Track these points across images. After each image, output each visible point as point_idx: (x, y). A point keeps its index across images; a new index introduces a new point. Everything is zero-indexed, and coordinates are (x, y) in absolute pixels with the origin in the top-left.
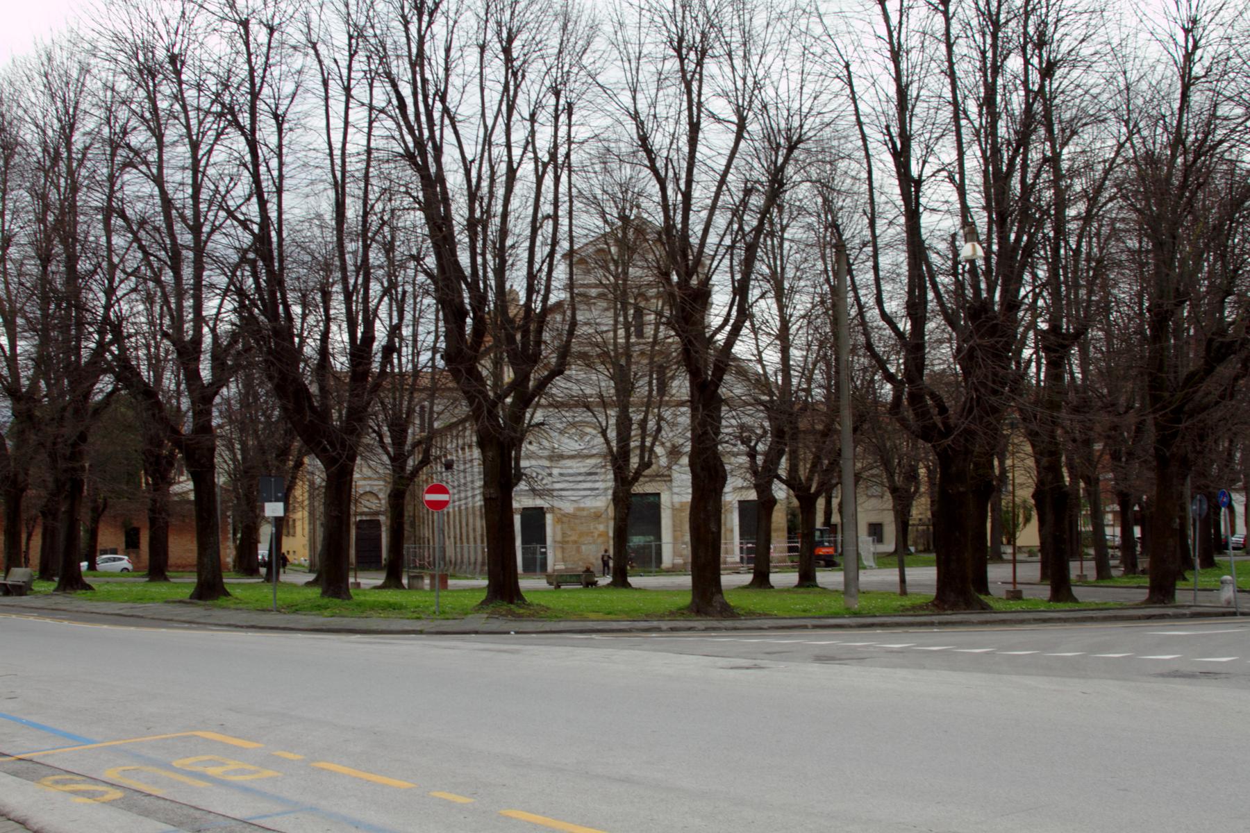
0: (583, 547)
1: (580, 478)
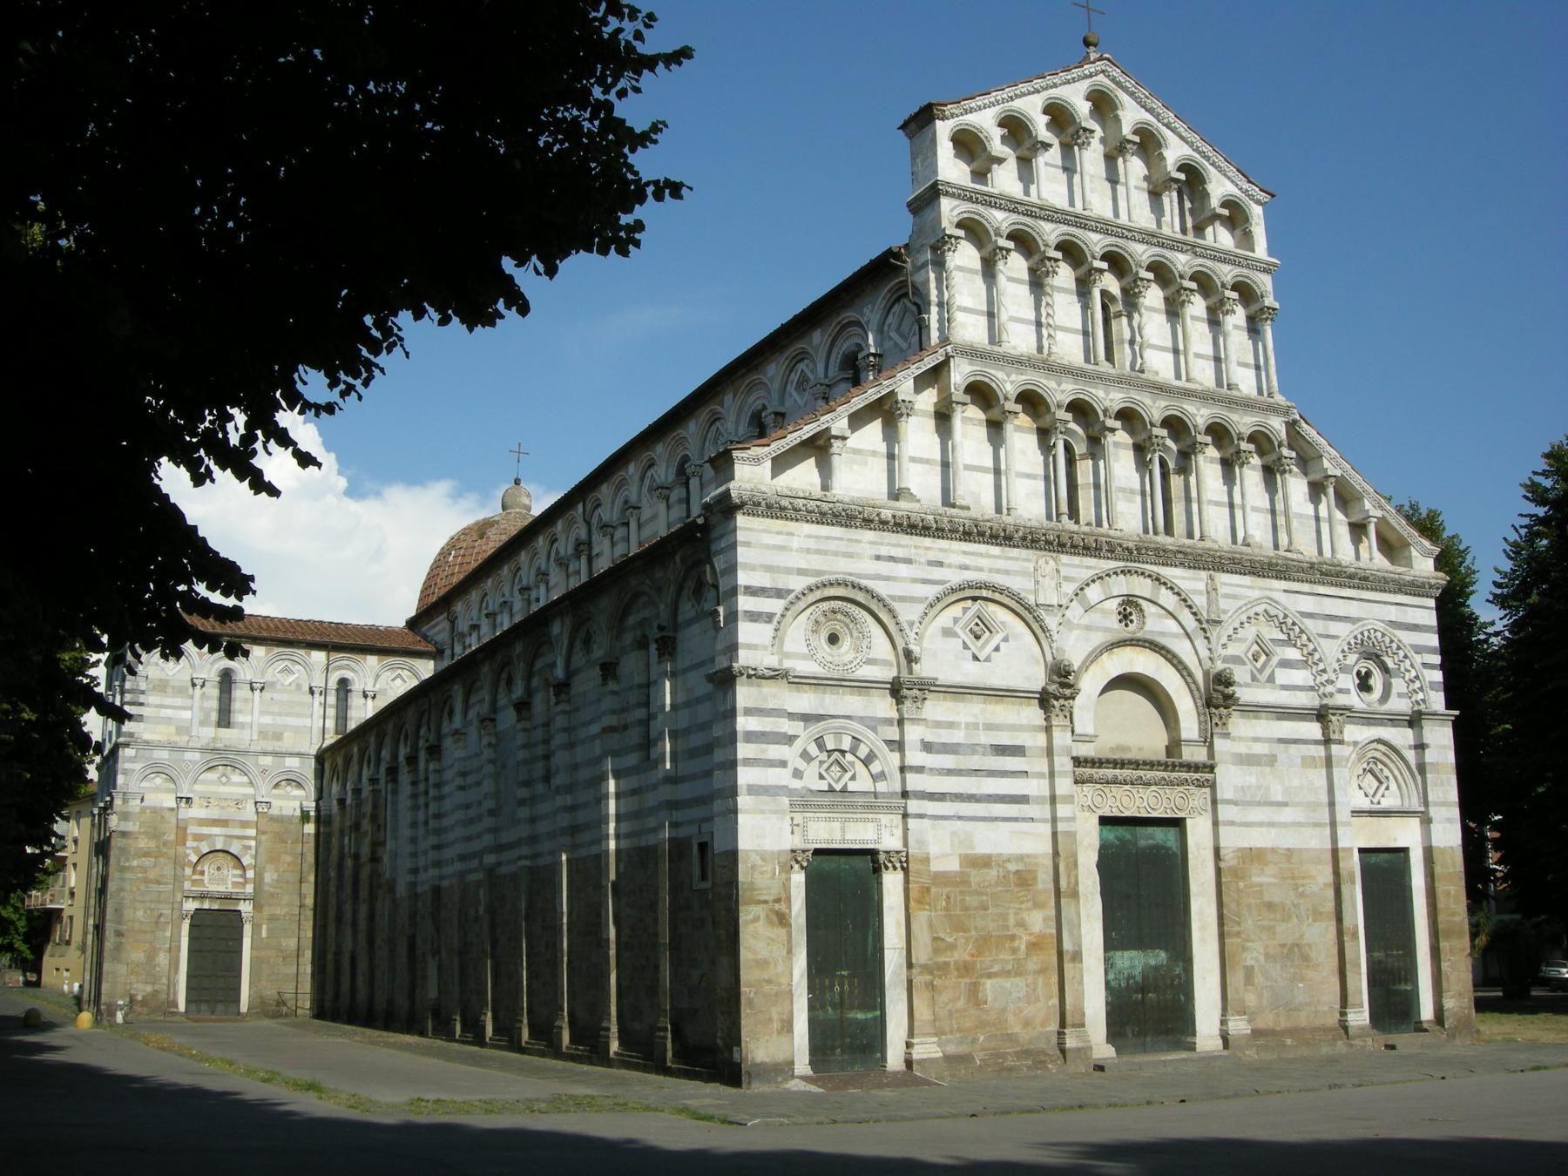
0: (989, 985)
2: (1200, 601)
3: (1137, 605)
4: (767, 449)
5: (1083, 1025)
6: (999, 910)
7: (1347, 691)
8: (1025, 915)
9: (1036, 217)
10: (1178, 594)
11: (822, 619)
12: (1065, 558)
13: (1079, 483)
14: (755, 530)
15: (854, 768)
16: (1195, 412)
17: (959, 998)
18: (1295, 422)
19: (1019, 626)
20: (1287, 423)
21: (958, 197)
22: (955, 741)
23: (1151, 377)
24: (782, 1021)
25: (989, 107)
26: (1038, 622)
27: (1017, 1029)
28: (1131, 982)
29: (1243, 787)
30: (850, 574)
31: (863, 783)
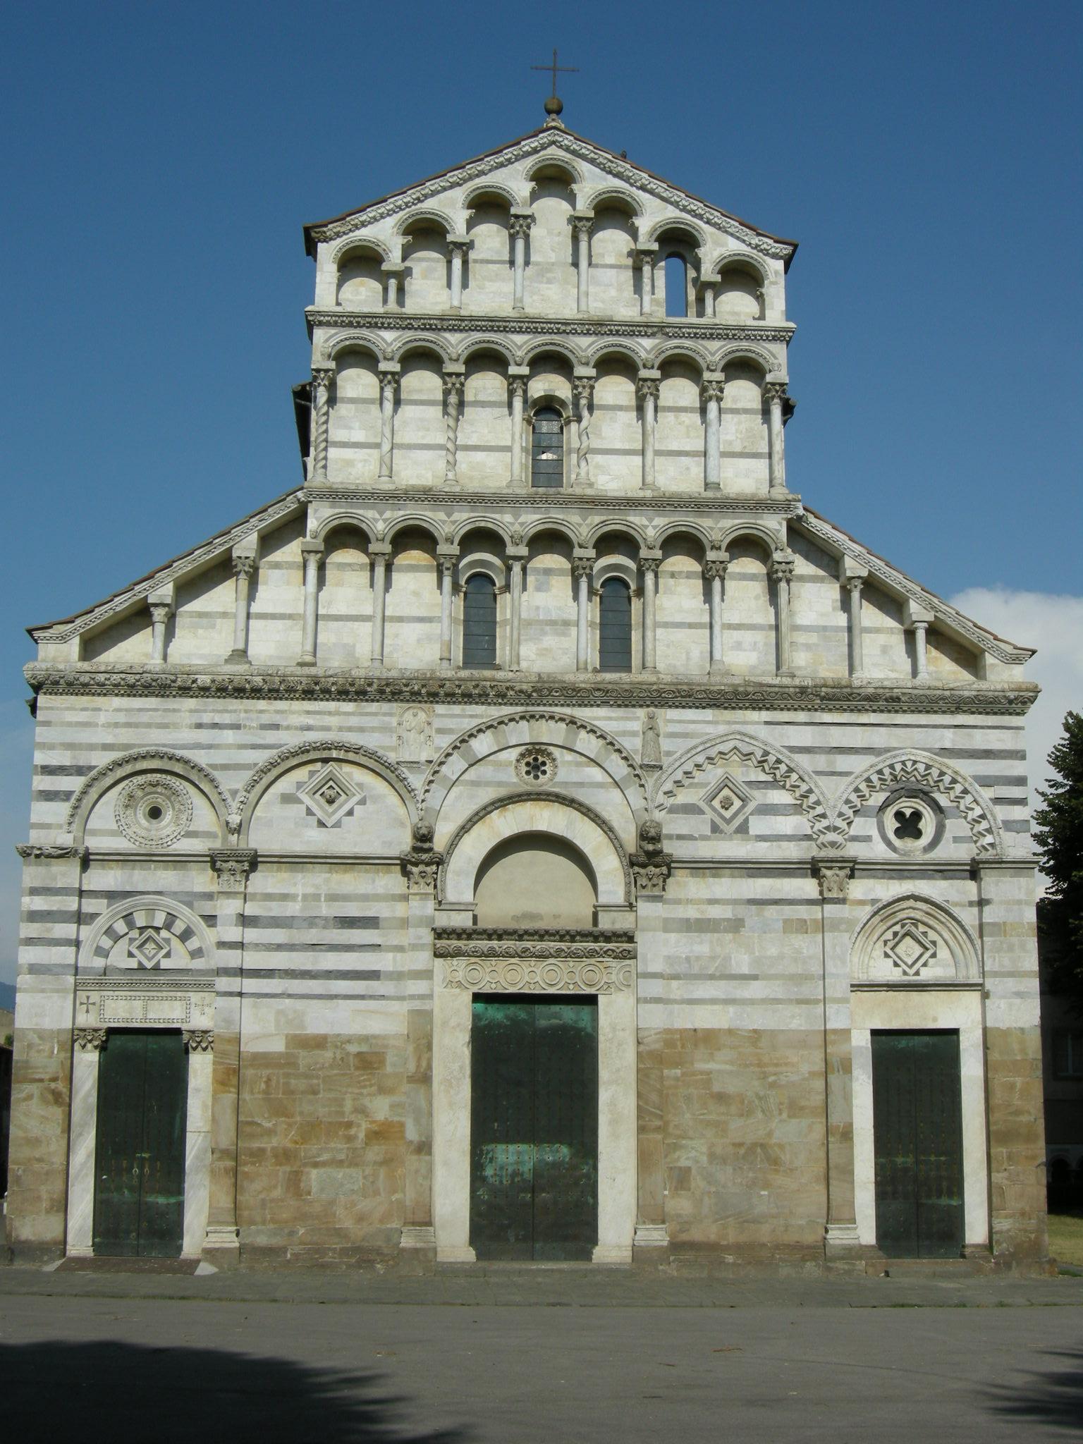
0: (314, 1176)
1: (313, 936)
2: (633, 745)
3: (549, 754)
4: (70, 625)
5: (429, 1223)
6: (331, 1095)
7: (868, 839)
8: (366, 1101)
9: (439, 330)
10: (602, 737)
11: (140, 793)
12: (440, 709)
13: (498, 620)
14: (57, 709)
15: (169, 945)
16: (647, 523)
17: (275, 1187)
18: (800, 518)
19: (378, 786)
20: (789, 521)
21: (335, 324)
22: (288, 914)
23: (578, 491)
24: (52, 1199)
25: (388, 215)
26: (401, 781)
27: (347, 1223)
28: (516, 1180)
29: (688, 959)
30: (164, 746)
31: (179, 958)
